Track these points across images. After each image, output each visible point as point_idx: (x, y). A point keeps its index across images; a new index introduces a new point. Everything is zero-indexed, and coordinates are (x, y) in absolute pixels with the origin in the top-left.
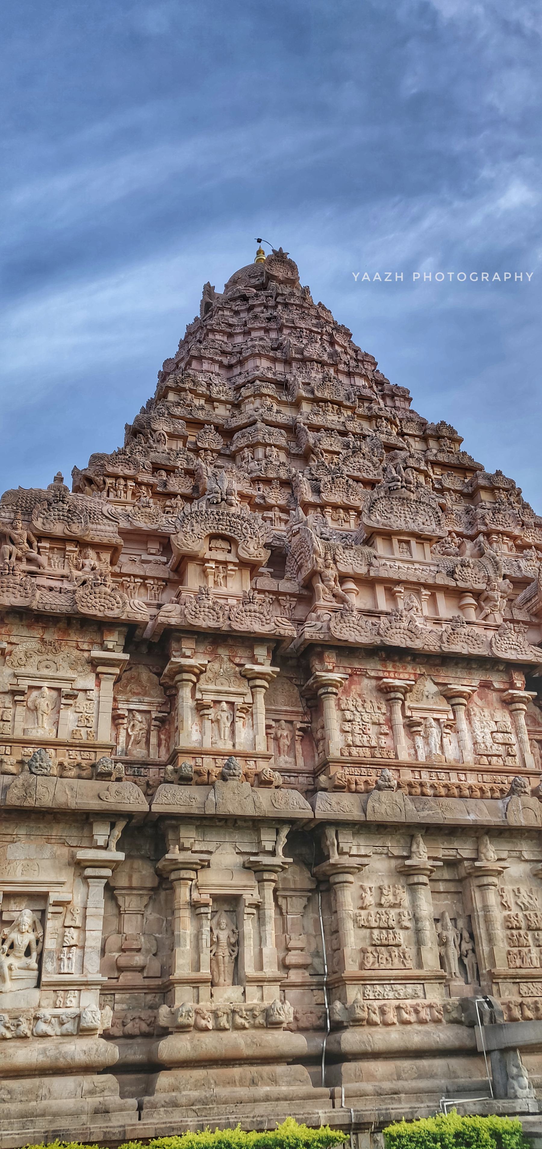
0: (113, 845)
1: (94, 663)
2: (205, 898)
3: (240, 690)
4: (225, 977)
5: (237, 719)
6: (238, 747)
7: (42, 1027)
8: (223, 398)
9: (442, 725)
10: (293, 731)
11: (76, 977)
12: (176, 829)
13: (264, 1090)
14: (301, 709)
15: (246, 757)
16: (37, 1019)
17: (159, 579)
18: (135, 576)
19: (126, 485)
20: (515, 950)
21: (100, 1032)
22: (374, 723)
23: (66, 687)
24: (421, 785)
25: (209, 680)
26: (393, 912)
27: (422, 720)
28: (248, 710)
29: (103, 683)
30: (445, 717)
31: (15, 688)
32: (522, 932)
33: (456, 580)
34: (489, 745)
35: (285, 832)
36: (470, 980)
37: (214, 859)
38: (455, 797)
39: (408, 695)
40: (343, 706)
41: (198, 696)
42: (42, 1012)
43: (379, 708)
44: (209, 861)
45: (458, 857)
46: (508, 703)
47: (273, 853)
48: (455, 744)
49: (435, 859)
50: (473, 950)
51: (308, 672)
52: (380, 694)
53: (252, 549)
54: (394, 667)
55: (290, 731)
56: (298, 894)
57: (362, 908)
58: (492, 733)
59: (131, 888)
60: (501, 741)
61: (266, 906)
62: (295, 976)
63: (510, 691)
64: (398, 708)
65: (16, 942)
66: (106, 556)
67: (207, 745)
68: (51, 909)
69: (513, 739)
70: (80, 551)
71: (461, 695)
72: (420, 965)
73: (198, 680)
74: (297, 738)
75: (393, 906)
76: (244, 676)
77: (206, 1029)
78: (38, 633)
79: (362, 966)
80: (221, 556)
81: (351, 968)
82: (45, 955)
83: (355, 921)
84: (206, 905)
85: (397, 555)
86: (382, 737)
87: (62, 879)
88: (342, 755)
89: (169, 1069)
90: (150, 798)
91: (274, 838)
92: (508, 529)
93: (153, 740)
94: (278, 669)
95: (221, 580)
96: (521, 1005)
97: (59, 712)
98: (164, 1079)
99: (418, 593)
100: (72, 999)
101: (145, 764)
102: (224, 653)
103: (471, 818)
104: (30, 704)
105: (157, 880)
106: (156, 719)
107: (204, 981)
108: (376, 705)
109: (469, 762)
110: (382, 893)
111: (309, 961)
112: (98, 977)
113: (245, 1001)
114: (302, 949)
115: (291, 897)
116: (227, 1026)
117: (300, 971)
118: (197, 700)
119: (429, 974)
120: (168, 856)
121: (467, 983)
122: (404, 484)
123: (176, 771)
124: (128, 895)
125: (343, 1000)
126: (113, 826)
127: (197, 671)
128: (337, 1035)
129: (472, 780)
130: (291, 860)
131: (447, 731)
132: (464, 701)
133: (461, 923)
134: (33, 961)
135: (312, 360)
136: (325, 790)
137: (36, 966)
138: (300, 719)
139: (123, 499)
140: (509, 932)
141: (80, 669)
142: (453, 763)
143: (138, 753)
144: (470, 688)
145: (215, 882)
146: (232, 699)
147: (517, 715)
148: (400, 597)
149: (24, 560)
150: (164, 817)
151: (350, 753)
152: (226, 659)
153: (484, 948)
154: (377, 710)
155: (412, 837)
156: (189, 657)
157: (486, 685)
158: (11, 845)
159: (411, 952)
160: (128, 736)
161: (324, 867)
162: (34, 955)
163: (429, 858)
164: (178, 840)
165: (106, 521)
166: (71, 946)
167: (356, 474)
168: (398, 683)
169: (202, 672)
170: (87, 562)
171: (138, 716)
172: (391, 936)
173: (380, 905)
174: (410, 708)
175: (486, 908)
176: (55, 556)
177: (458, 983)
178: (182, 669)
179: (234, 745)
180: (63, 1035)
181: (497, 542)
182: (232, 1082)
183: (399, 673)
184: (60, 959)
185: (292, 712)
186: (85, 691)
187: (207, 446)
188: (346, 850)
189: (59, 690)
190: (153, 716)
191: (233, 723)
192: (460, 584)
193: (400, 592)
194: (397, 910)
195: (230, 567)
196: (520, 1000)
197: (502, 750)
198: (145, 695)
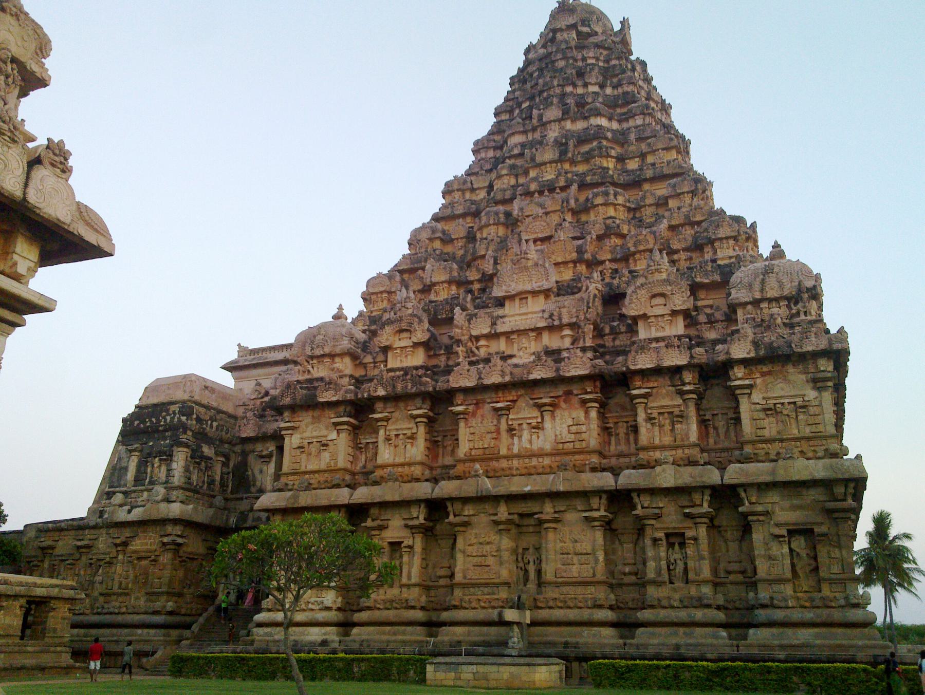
3: (410, 426)
6: (407, 460)
7: (310, 606)
8: (481, 186)
13: (400, 637)
15: (410, 464)
18: (370, 363)
20: (563, 567)
22: (488, 433)
23: (324, 440)
25: (393, 423)
26: (488, 548)
28: (413, 437)
33: (554, 320)
34: (563, 435)
37: (390, 523)
40: (469, 425)
41: (388, 433)
43: (492, 422)
46: (584, 402)
54: (503, 394)
57: (469, 545)
58: (569, 426)
66: (347, 360)
67: (391, 461)
69: (584, 428)
71: (545, 405)
75: (488, 543)
77: (379, 609)
78: (310, 413)
79: (465, 578)
80: (403, 343)
81: (458, 577)
85: (518, 312)
88: (465, 455)
91: (418, 510)
98: (355, 630)
102: (401, 405)
103: (527, 489)
122: (523, 256)
129: (547, 461)
131: (534, 430)
132: (550, 408)
135: (550, 122)
143: (370, 467)
146: (405, 432)
150: (361, 505)
152: (403, 408)
155: (499, 502)
160: (366, 457)
163: (509, 514)
165: (344, 338)
168: (499, 405)
169: (389, 419)
173: (481, 543)
174: (512, 419)
182: (384, 633)
194: (491, 546)
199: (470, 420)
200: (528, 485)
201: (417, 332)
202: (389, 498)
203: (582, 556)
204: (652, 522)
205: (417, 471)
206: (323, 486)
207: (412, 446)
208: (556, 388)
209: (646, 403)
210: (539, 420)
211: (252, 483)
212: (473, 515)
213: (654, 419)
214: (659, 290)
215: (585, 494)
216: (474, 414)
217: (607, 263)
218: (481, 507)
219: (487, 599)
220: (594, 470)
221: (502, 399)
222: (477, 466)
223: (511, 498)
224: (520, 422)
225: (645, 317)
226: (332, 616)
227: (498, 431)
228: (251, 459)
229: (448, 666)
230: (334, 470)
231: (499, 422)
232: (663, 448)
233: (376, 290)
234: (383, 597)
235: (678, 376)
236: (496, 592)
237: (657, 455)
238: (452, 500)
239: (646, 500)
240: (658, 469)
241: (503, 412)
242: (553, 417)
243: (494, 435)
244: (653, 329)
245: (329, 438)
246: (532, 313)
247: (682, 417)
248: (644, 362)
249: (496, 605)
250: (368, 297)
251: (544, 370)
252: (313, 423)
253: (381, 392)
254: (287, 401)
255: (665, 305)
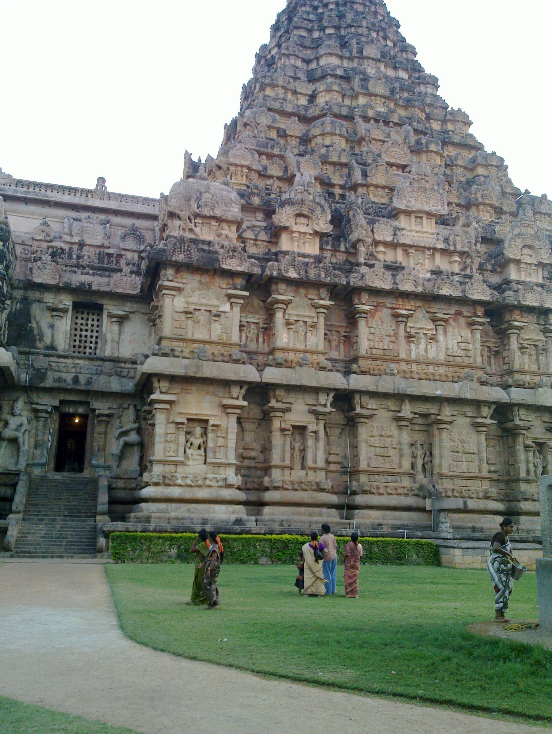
0: (241, 397)
1: (230, 297)
2: (288, 427)
3: (311, 314)
4: (297, 466)
5: (308, 331)
7: (208, 482)
8: (304, 92)
9: (428, 338)
10: (339, 337)
11: (223, 461)
12: (274, 390)
14: (345, 325)
15: (313, 353)
16: (206, 478)
17: (264, 241)
19: (242, 171)
21: (236, 486)
22: (387, 335)
23: (214, 311)
24: (411, 372)
26: (389, 440)
27: (416, 335)
28: (314, 326)
29: (234, 308)
30: (430, 332)
31: (186, 310)
32: (459, 454)
33: (449, 245)
34: (455, 350)
35: (332, 395)
36: (427, 475)
37: (293, 407)
38: (430, 380)
39: (409, 319)
40: (370, 325)
41: (287, 317)
42: (208, 476)
43: (391, 326)
44: (290, 408)
45: (429, 413)
46: (471, 324)
47: (325, 406)
48: (434, 349)
49: (415, 413)
50: (431, 461)
51: (351, 304)
52: (393, 318)
53: (322, 225)
54: (403, 302)
55: (337, 336)
56: (336, 426)
57: (371, 436)
58: (458, 342)
59: (249, 418)
60: (463, 348)
61: (320, 433)
62: (333, 467)
63: (473, 318)
64: (402, 327)
65: (194, 443)
66: (234, 228)
67: (291, 346)
68: (210, 428)
69: (471, 347)
70: (219, 225)
71: (442, 320)
72: (400, 467)
73: (287, 308)
74: (341, 341)
76: (313, 306)
77: (287, 489)
78: (197, 277)
79: (368, 465)
80: (303, 229)
81: (363, 465)
82: (208, 450)
83: (366, 442)
84: (289, 430)
85: (413, 228)
86: (391, 343)
87: (216, 414)
88: (367, 353)
89: (269, 505)
90: (261, 372)
92: (491, 202)
93: (261, 340)
94: (333, 303)
95: (301, 244)
96: (453, 490)
97: (210, 324)
98: (267, 510)
99: (424, 252)
100: (222, 470)
101: (256, 353)
102: (302, 291)
103: (438, 393)
104: (195, 319)
105: (263, 415)
106: (262, 328)
107: (286, 467)
108: (389, 325)
109: (441, 360)
110: (383, 429)
111: (340, 460)
112: (234, 462)
113: (307, 478)
114: (337, 454)
115: (333, 427)
116: (298, 488)
117: (336, 465)
118: (286, 319)
119: (404, 471)
120: (270, 405)
121: (425, 477)
122: (423, 177)
123: (274, 359)
124: (248, 422)
125: (358, 481)
126: (241, 388)
127: (286, 302)
128: (353, 497)
129: (442, 370)
130: (334, 410)
131: (431, 341)
133: (425, 447)
134: (202, 451)
136: (355, 373)
137: (204, 454)
138: (344, 330)
139: (240, 182)
140: (452, 453)
141: (222, 299)
142: (432, 361)
143: (252, 346)
144: (448, 316)
145: (293, 419)
146: (306, 320)
147: (476, 333)
148: (412, 256)
149: (187, 230)
150: (268, 385)
151: (371, 352)
152: (303, 295)
153: (437, 461)
154: (389, 328)
156: (281, 294)
157: (459, 313)
158: (188, 395)
159: (396, 459)
160: (247, 337)
161: (352, 414)
162: (203, 449)
163: (411, 412)
164: (275, 397)
165: (234, 205)
166: (221, 446)
167: (393, 160)
169: (289, 303)
170: (223, 232)
171: (253, 326)
172: (386, 452)
173: (382, 436)
174: (410, 327)
175: (440, 440)
176: (204, 228)
177: (420, 477)
178: (278, 302)
179: (306, 346)
180: (219, 487)
181: (483, 211)
182: (300, 514)
183: (406, 305)
184: (216, 452)
185: (340, 326)
186: (225, 312)
187: (292, 134)
188: (365, 406)
189: (210, 311)
190: (261, 326)
191: (306, 333)
192: (452, 248)
193: (412, 253)
195: (308, 236)
196: (453, 487)
197: (462, 353)
198: (256, 313)
199: (370, 320)
200: (437, 390)
201: (320, 221)
202: (306, 382)
203: (470, 455)
204: (523, 432)
205: (322, 359)
206: (219, 359)
207: (312, 334)
208: (450, 306)
209: (519, 334)
210: (434, 333)
211: (38, 337)
212: (376, 409)
213: (527, 348)
214: (529, 242)
215: (477, 404)
216: (373, 316)
217: (454, 205)
218: (384, 403)
219: (393, 486)
220: (483, 383)
221: (401, 307)
222: (393, 366)
223: (415, 398)
224: (417, 331)
225: (518, 262)
226: (241, 496)
227: (396, 335)
228: (36, 310)
229: (475, 551)
230: (230, 344)
231: (398, 327)
232: (532, 373)
233: (238, 162)
234: (289, 479)
235: (543, 317)
236: (399, 481)
237: (527, 378)
238: (361, 393)
239: (523, 414)
240: (540, 389)
241: (405, 319)
242: (445, 332)
243: (393, 339)
244: (523, 274)
245: (222, 310)
246: (428, 233)
247: (543, 350)
248: (531, 300)
249: (402, 492)
250: (225, 167)
251: (452, 288)
252: (199, 289)
253: (293, 274)
254: (180, 257)
255: (531, 256)
